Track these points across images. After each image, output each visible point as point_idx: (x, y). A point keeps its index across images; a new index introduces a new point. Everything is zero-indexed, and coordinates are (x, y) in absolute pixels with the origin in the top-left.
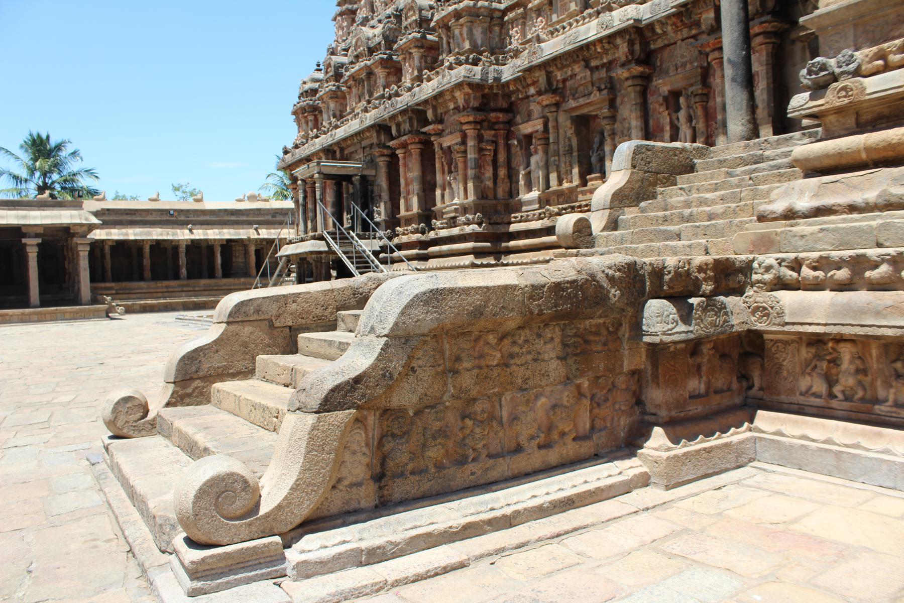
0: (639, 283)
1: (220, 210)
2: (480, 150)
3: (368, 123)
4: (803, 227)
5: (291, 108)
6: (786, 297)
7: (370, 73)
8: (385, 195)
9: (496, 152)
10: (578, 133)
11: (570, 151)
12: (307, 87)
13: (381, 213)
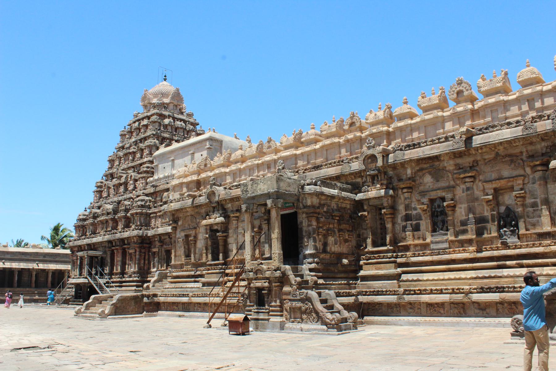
0: (143, 296)
1: (16, 252)
2: (140, 255)
3: (105, 240)
4: (166, 290)
5: (73, 224)
6: (161, 298)
7: (107, 221)
8: (109, 264)
9: (145, 256)
10: (166, 254)
11: (164, 259)
12: (81, 217)
13: (107, 270)
